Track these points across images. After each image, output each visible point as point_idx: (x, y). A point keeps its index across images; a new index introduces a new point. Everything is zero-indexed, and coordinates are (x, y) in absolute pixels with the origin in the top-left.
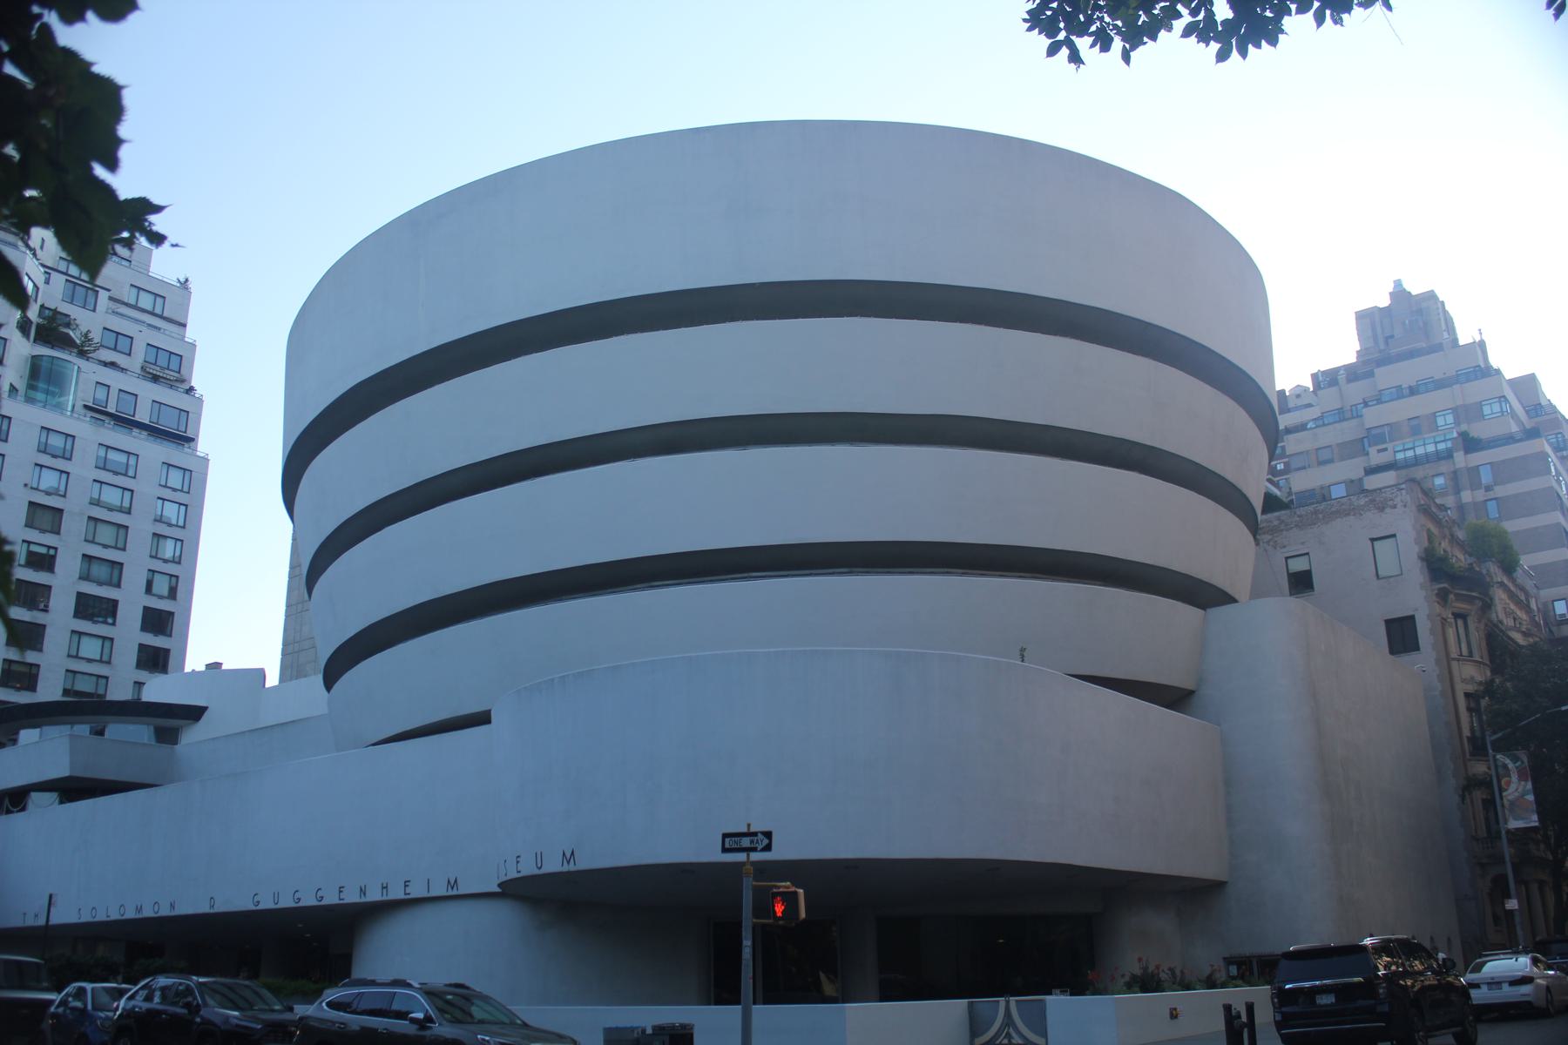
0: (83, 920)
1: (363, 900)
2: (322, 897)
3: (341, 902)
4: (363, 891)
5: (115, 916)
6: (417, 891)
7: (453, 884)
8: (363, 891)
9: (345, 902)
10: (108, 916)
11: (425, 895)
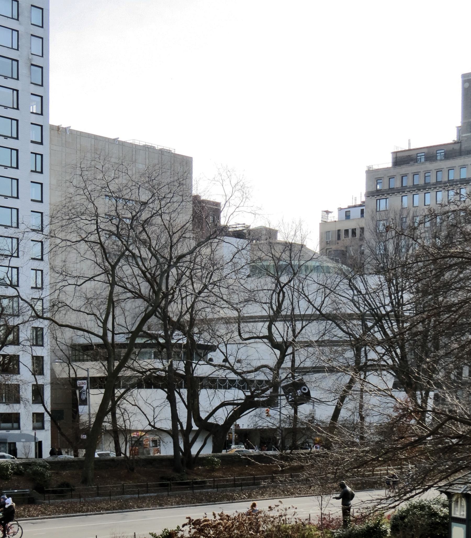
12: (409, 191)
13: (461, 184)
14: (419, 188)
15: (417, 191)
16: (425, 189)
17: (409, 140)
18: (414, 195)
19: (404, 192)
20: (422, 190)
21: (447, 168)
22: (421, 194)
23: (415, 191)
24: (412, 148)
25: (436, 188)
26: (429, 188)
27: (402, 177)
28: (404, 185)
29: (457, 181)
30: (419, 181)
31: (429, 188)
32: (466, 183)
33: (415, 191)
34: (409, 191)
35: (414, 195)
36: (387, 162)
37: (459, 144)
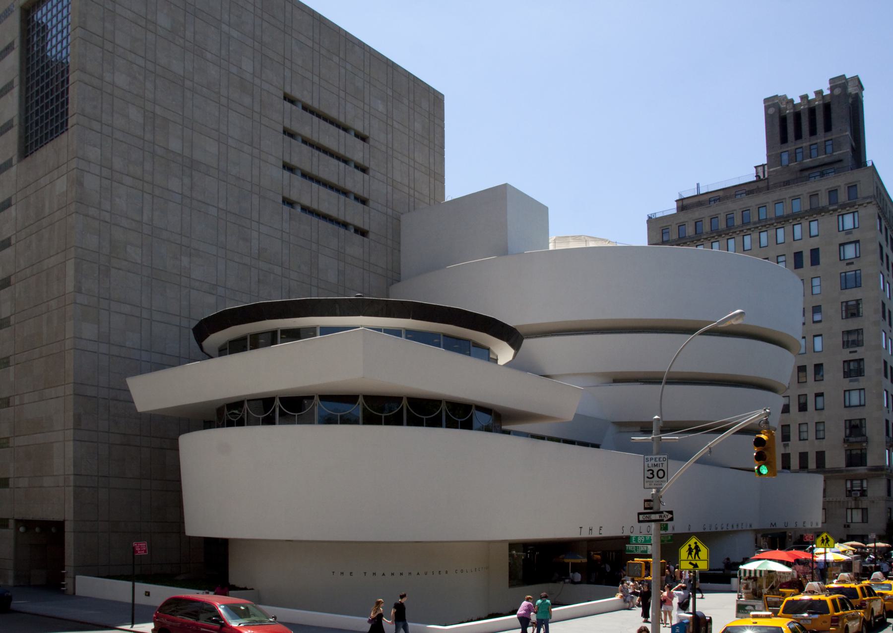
12: (706, 239)
13: (777, 223)
15: (716, 237)
16: (728, 234)
18: (712, 243)
19: (699, 240)
20: (723, 236)
21: (756, 205)
23: (714, 237)
26: (733, 233)
29: (771, 219)
31: (733, 233)
33: (714, 237)
34: (706, 239)
36: (670, 208)
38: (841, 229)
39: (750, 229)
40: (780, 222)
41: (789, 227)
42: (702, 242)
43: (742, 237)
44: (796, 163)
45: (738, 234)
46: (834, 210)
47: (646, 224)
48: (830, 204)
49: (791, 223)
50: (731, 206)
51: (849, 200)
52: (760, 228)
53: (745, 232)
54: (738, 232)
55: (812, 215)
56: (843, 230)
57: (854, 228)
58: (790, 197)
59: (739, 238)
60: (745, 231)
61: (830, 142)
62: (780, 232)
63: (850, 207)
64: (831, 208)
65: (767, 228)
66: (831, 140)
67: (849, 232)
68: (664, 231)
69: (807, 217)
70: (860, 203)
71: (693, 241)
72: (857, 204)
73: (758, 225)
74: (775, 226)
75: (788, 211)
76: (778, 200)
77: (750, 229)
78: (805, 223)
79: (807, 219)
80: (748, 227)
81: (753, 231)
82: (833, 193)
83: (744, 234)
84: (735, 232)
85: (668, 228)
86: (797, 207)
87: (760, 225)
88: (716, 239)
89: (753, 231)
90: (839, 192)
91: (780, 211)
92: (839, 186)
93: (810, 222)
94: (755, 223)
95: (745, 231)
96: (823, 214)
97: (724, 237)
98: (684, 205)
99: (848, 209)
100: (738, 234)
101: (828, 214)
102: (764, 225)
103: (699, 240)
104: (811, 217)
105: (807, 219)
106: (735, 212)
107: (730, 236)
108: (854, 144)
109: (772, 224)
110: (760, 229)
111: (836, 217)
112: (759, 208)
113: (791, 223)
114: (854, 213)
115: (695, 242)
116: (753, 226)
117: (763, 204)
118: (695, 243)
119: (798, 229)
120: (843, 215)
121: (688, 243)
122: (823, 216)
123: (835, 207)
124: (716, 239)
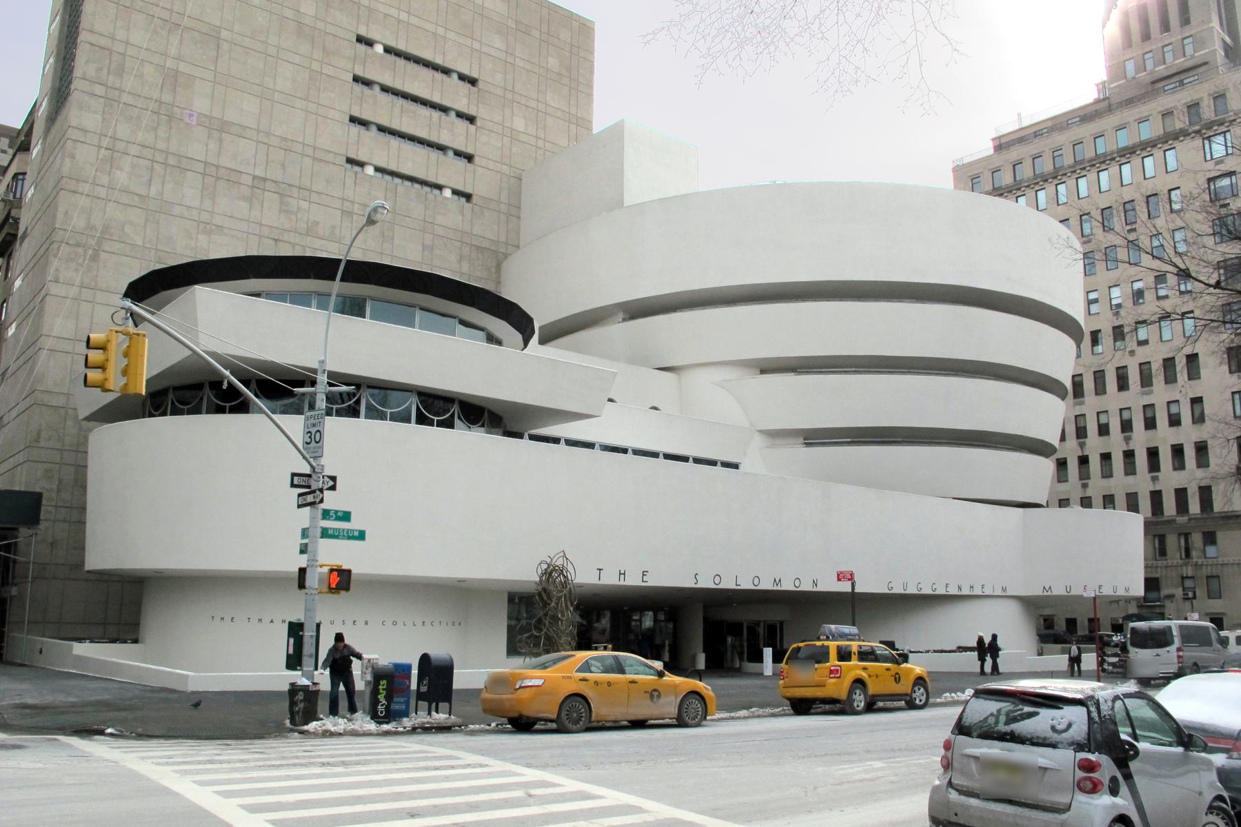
0: (701, 585)
1: (960, 593)
2: (936, 589)
3: (947, 593)
4: (960, 588)
5: (746, 584)
6: (988, 592)
7: (1004, 590)
8: (960, 588)
9: (949, 593)
10: (739, 585)
11: (991, 593)
13: (1120, 156)
14: (1045, 178)
15: (1041, 183)
17: (1019, 115)
19: (1019, 189)
20: (1050, 180)
21: (1091, 135)
22: (1050, 188)
23: (1037, 183)
24: (1024, 125)
25: (1075, 172)
27: (1014, 166)
28: (1018, 179)
29: (1112, 153)
30: (1046, 166)
32: (1131, 153)
33: (1037, 183)
35: (1036, 191)
37: (1107, 102)
38: (1208, 157)
39: (1084, 168)
40: (1124, 156)
41: (1136, 161)
42: (1023, 191)
43: (1075, 180)
44: (1144, 73)
45: (1070, 177)
46: (1198, 132)
47: (952, 174)
48: (1190, 124)
49: (1139, 155)
50: (1060, 139)
51: (1216, 116)
52: (1097, 165)
53: (1079, 174)
54: (1069, 174)
55: (1167, 142)
56: (1212, 159)
57: (1227, 154)
58: (1135, 120)
59: (1071, 182)
60: (1078, 171)
61: (1190, 40)
62: (1126, 169)
63: (1219, 125)
64: (1190, 130)
65: (1108, 164)
66: (1191, 36)
67: (1220, 161)
68: (975, 181)
69: (1159, 146)
70: (1232, 118)
71: (1011, 191)
72: (1227, 120)
73: (1095, 162)
74: (1118, 161)
75: (1135, 140)
76: (1119, 126)
77: (1084, 168)
78: (1158, 153)
79: (1160, 148)
80: (1082, 167)
81: (1088, 171)
82: (1193, 107)
83: (1078, 176)
84: (1066, 174)
85: (979, 177)
86: (1147, 132)
87: (1097, 161)
88: (1042, 185)
89: (1088, 171)
90: (1201, 105)
91: (1124, 140)
92: (1202, 99)
93: (1165, 151)
94: (1091, 160)
95: (1078, 171)
96: (1182, 138)
97: (1051, 182)
98: (1002, 145)
99: (1215, 128)
100: (1070, 177)
101: (1188, 138)
102: (1101, 162)
103: (1019, 189)
104: (1166, 145)
105: (1160, 148)
106: (1063, 147)
107: (1060, 180)
108: (1228, 39)
109: (1113, 159)
110: (1098, 168)
111: (1201, 140)
112: (1095, 138)
113: (1139, 155)
114: (1224, 133)
115: (1014, 192)
116: (1088, 165)
117: (1099, 133)
118: (1015, 194)
119: (1149, 162)
120: (1209, 138)
121: (1005, 194)
122: (1182, 141)
123: (1197, 128)
124: (1042, 185)
